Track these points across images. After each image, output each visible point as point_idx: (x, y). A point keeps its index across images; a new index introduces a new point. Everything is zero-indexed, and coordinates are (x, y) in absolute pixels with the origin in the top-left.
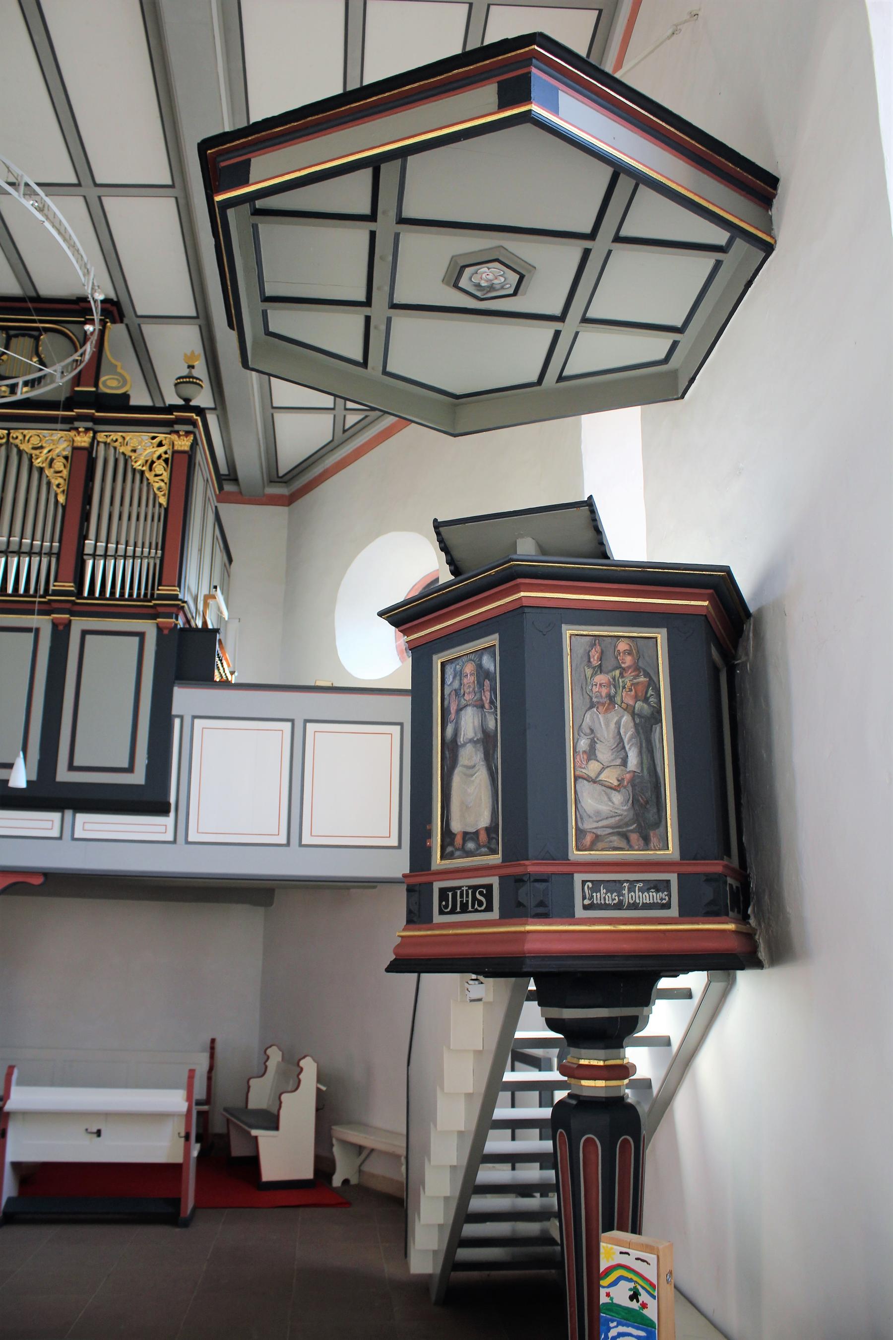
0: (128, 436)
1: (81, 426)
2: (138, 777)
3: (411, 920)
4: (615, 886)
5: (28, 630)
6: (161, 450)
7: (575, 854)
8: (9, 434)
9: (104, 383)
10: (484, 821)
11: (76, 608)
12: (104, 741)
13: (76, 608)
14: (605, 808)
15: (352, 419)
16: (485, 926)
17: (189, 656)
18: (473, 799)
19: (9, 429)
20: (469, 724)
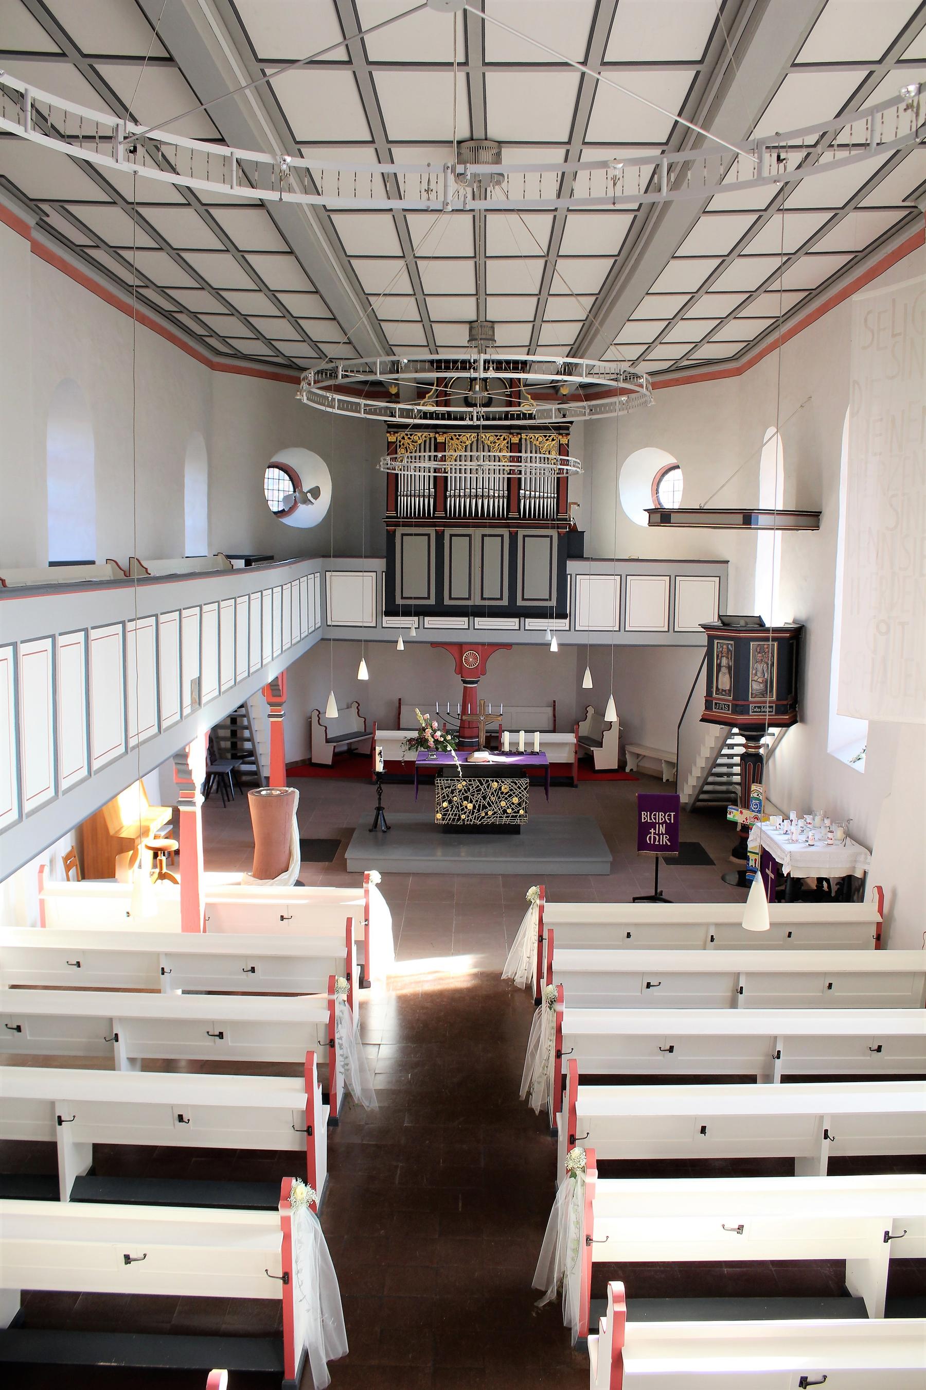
3: (706, 708)
4: (759, 707)
7: (750, 699)
10: (728, 688)
12: (537, 585)
14: (758, 688)
16: (727, 714)
17: (572, 545)
18: (725, 681)
20: (724, 661)
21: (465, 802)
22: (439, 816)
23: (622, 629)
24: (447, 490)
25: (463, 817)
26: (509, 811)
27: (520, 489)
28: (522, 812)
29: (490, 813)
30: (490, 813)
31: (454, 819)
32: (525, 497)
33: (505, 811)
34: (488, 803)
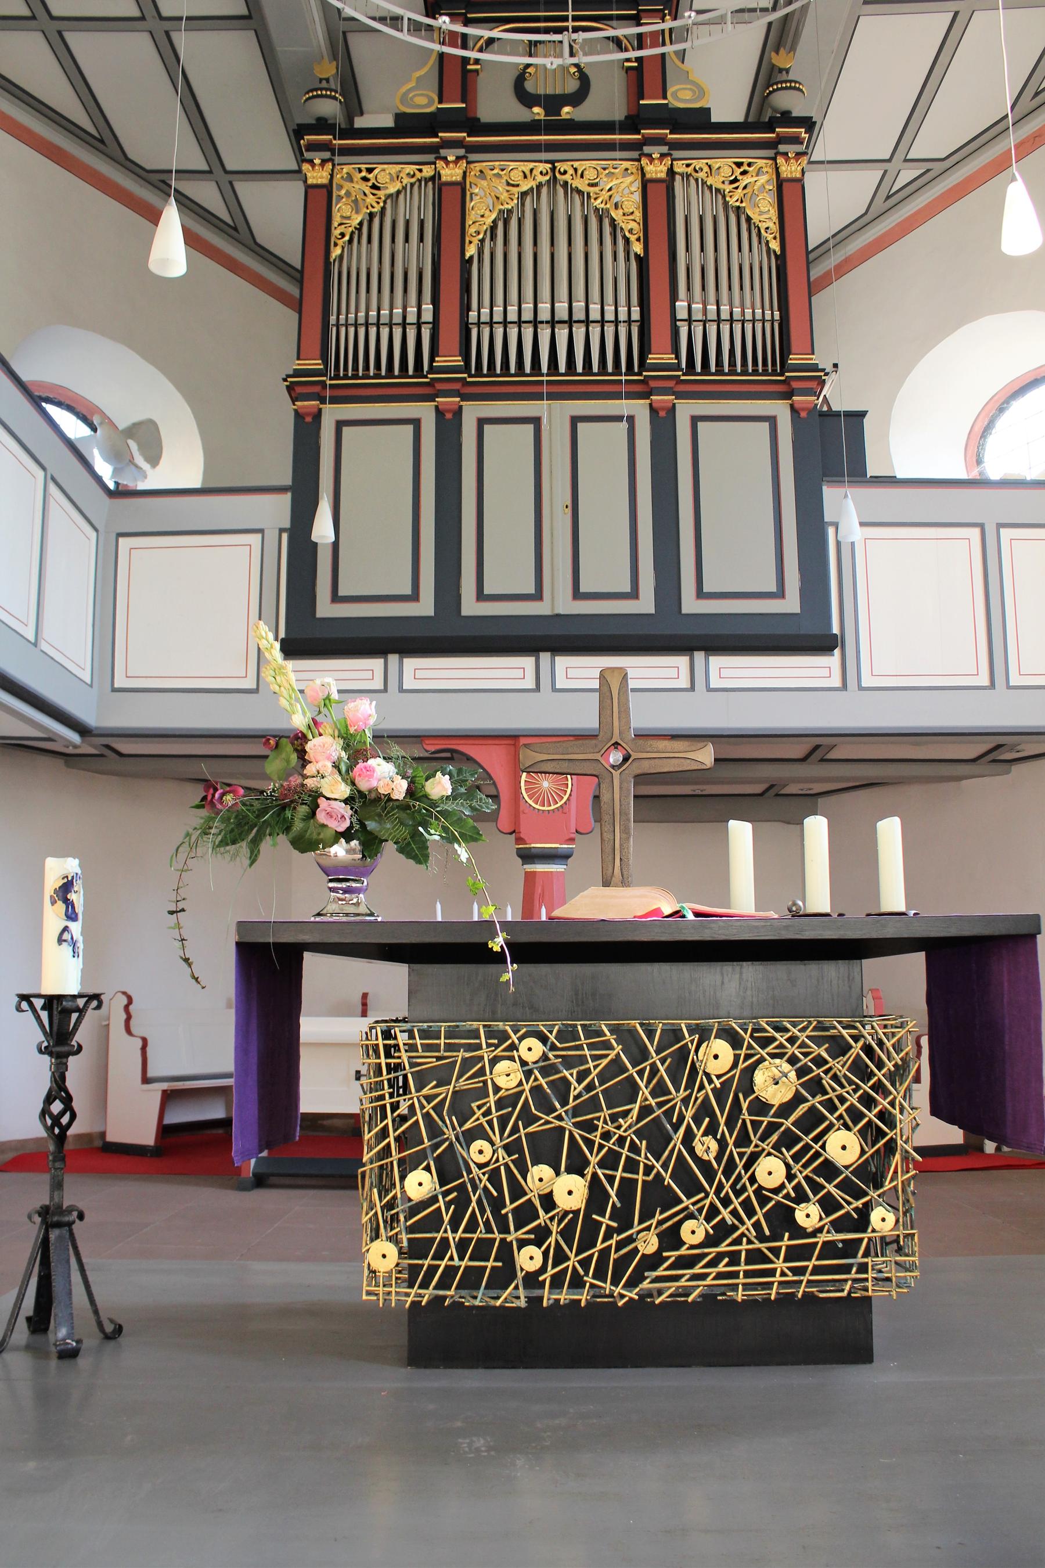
0: (716, 164)
1: (656, 151)
2: (791, 604)
5: (619, 419)
6: (763, 179)
8: (553, 169)
9: (675, 94)
11: (681, 388)
12: (738, 558)
13: (681, 388)
15: (907, 175)
17: (832, 447)
19: (552, 162)
21: (543, 1171)
22: (383, 1255)
23: (1000, 680)
24: (469, 309)
25: (529, 1258)
26: (808, 1215)
27: (674, 297)
28: (882, 1220)
29: (694, 1232)
30: (694, 1232)
31: (471, 1280)
32: (689, 321)
33: (783, 1220)
34: (682, 1172)
